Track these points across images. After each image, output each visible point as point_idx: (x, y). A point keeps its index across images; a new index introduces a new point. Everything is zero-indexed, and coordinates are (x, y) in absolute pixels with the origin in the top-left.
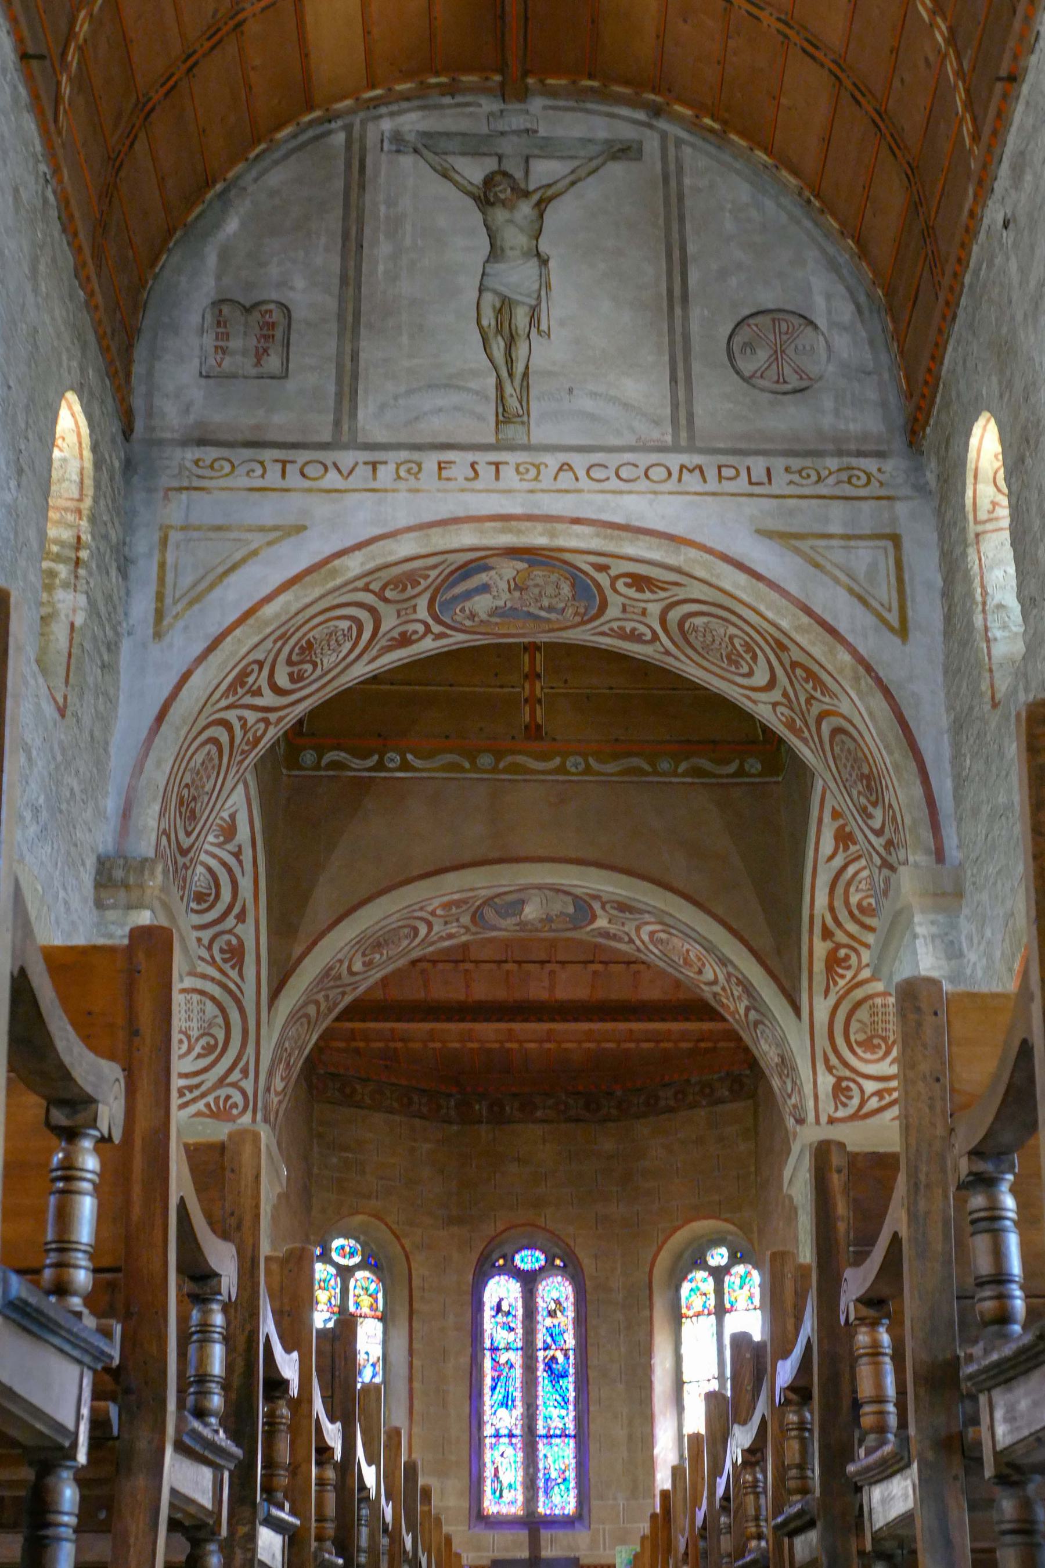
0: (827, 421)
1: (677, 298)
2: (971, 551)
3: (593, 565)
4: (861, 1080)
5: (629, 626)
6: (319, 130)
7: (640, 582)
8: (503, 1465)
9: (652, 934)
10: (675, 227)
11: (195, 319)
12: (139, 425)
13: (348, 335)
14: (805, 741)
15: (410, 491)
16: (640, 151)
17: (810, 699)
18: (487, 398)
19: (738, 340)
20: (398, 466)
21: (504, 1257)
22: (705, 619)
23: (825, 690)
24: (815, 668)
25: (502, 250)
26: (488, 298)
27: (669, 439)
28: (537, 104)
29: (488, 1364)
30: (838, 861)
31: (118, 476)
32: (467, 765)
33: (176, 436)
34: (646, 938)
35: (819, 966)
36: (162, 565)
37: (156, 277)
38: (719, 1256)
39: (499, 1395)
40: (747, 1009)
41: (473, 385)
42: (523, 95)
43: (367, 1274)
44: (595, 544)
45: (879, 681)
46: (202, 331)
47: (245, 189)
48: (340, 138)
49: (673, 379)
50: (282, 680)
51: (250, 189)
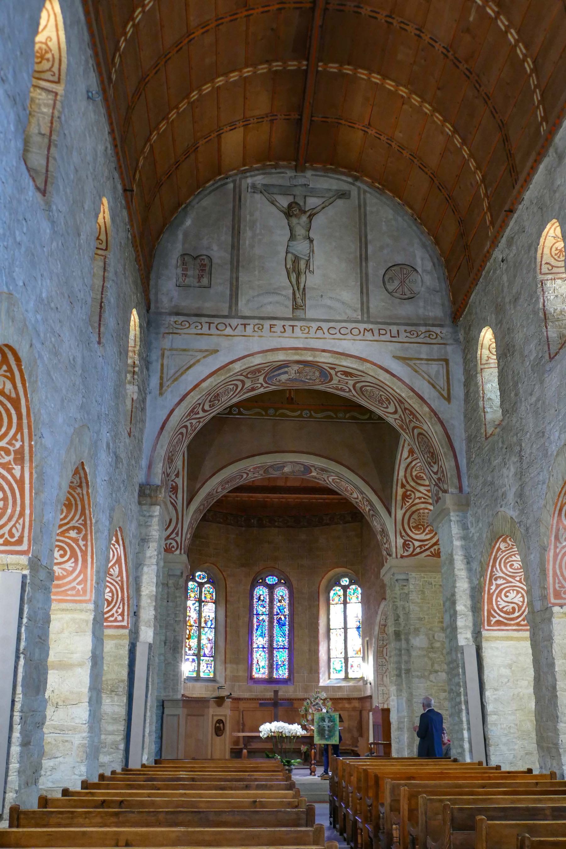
0: (421, 311)
1: (364, 258)
2: (479, 375)
4: (414, 541)
5: (340, 387)
6: (222, 182)
7: (346, 374)
8: (260, 659)
9: (333, 479)
10: (363, 228)
11: (174, 262)
12: (152, 306)
13: (235, 270)
14: (407, 433)
15: (259, 336)
16: (350, 194)
17: (410, 421)
18: (289, 298)
19: (387, 277)
20: (254, 326)
21: (262, 579)
23: (417, 419)
24: (415, 412)
25: (295, 236)
26: (290, 256)
27: (360, 317)
28: (309, 173)
30: (409, 460)
31: (145, 330)
32: (264, 413)
33: (167, 311)
34: (331, 480)
35: (399, 498)
36: (162, 365)
37: (159, 243)
38: (345, 581)
39: (259, 633)
40: (370, 510)
41: (284, 293)
42: (303, 170)
43: (209, 585)
44: (331, 360)
45: (439, 418)
46: (177, 267)
47: (193, 207)
48: (231, 186)
49: (362, 292)
50: (207, 407)
51: (196, 206)
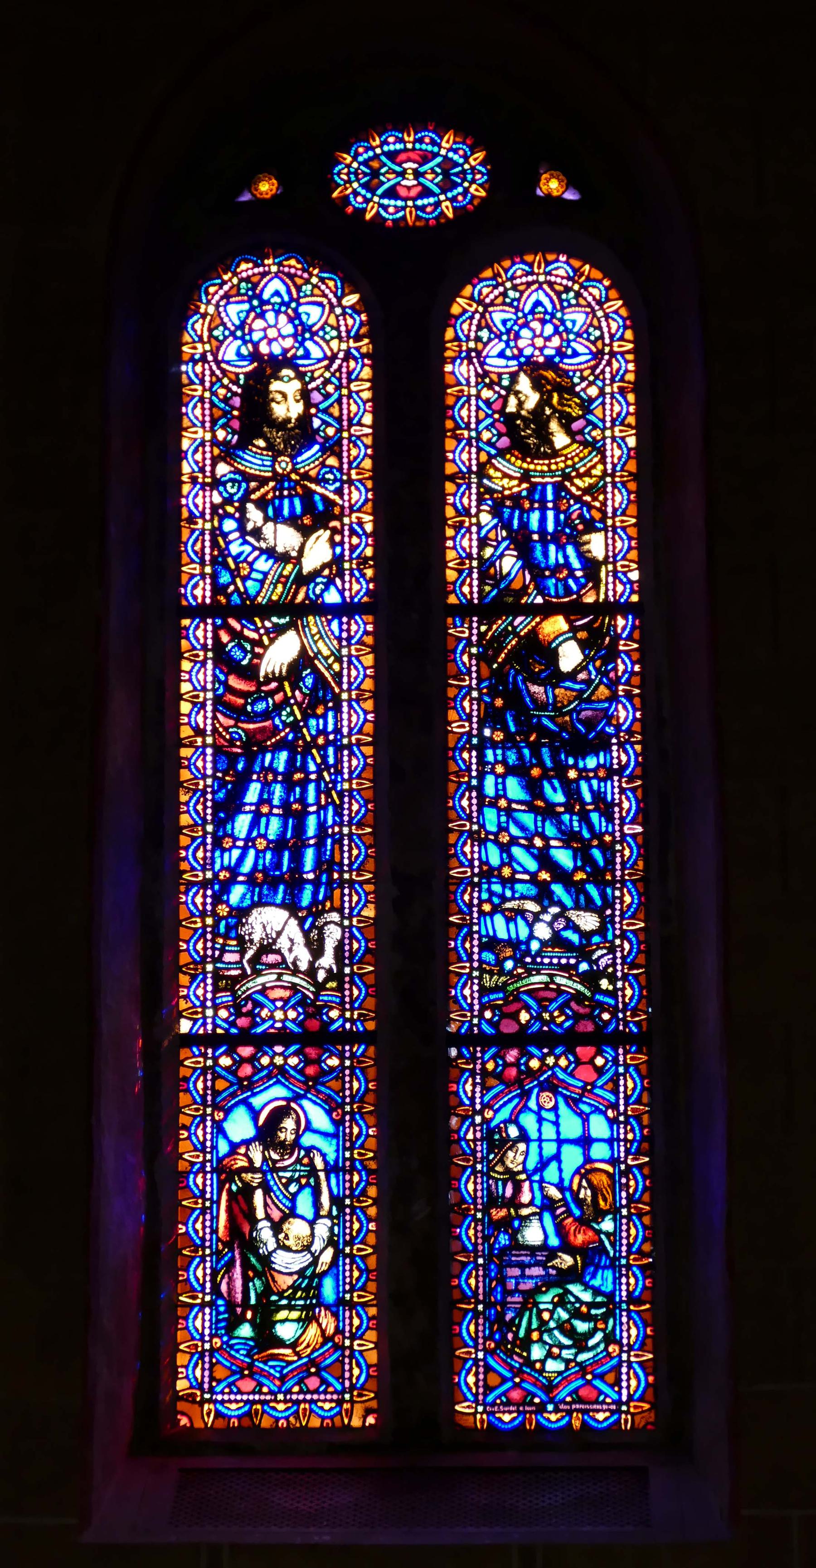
29: (197, 678)
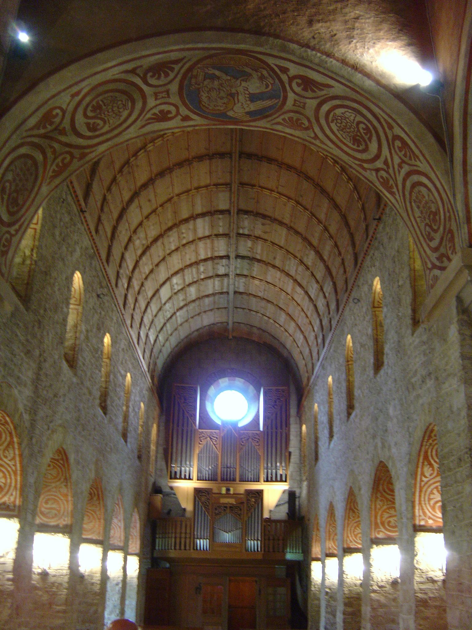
3: (191, 119)
22: (122, 119)
